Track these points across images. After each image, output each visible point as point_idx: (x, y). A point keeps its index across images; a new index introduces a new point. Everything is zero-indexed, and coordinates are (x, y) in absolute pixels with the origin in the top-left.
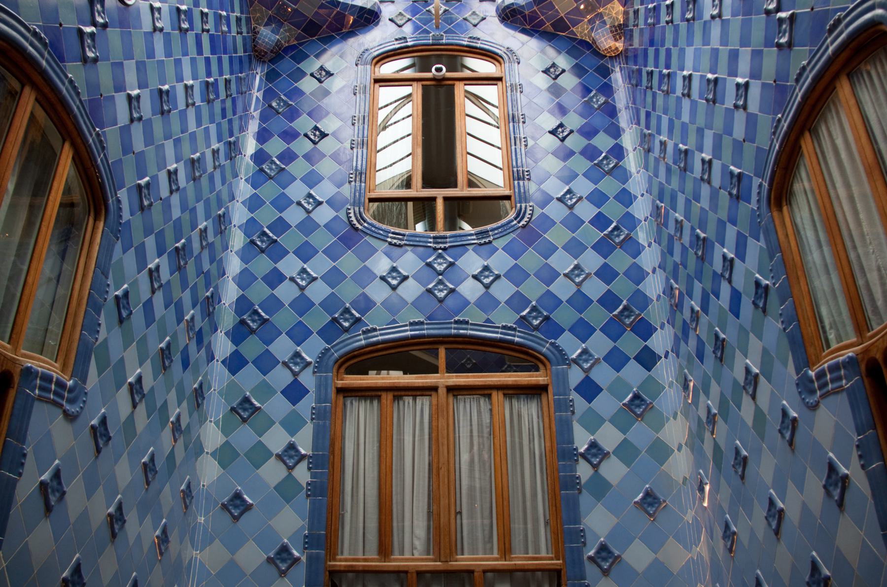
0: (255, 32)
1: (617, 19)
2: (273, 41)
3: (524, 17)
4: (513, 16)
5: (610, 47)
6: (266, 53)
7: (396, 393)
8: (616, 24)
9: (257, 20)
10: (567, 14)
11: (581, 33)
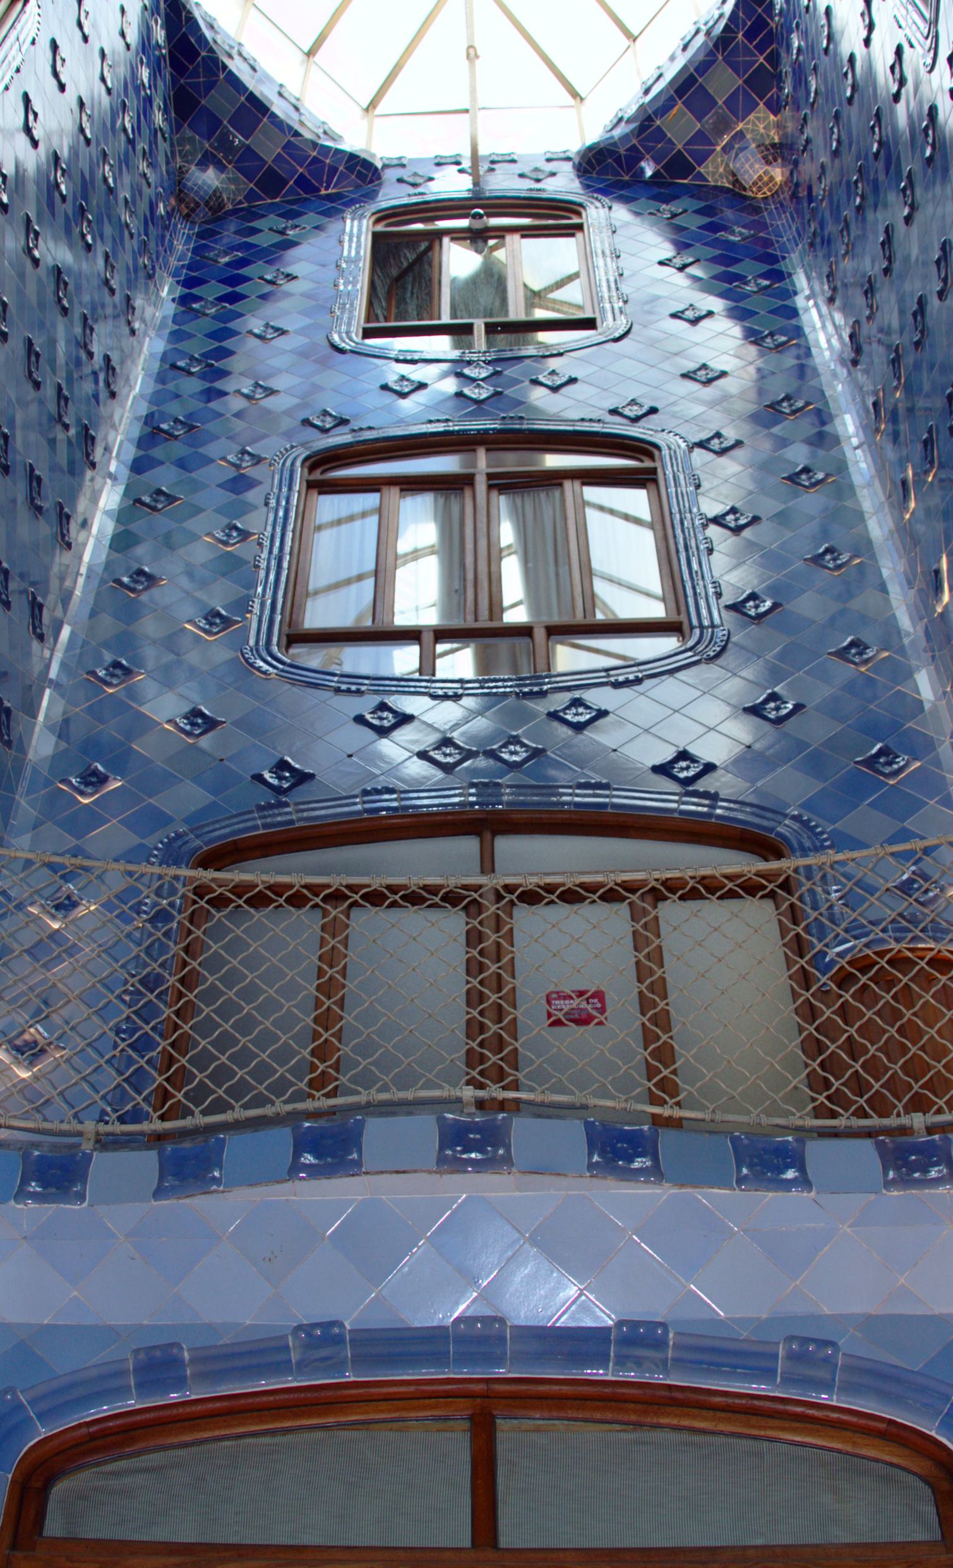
0: (181, 171)
1: (768, 136)
2: (209, 186)
3: (618, 160)
4: (599, 162)
5: (760, 178)
6: (198, 205)
7: (404, 487)
8: (767, 142)
9: (186, 156)
10: (687, 144)
11: (714, 174)
